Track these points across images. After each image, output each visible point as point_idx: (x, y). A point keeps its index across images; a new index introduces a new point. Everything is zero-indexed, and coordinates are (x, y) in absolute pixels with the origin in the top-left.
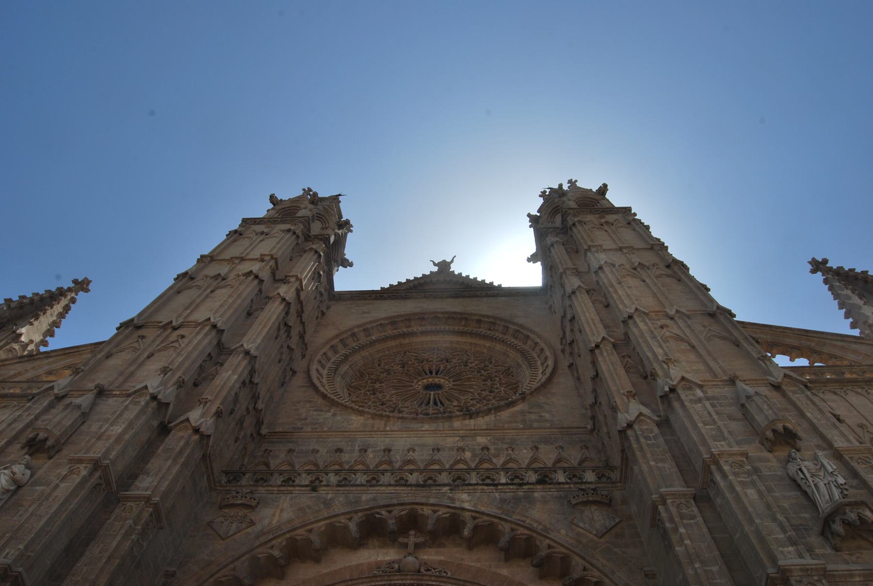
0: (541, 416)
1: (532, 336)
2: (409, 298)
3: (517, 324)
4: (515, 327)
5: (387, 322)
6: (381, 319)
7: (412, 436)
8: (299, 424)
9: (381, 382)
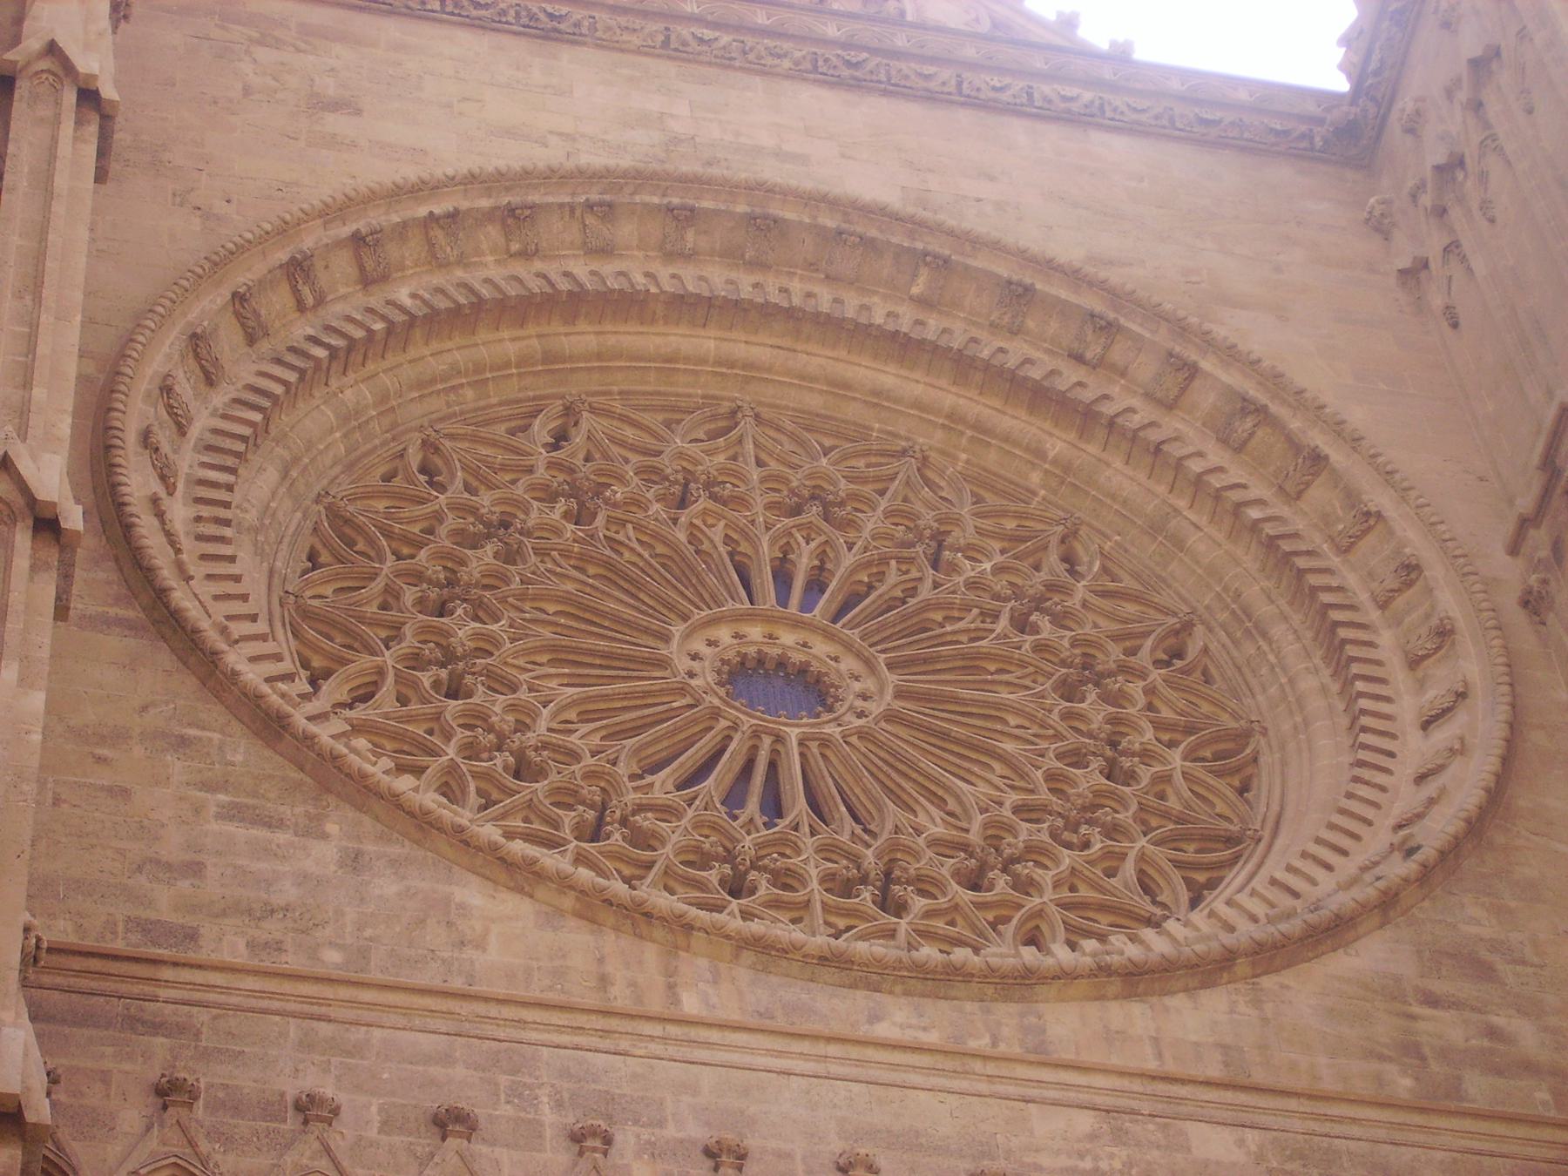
0: (1493, 1033)
1: (1337, 456)
2: (574, 38)
3: (1251, 365)
4: (1232, 378)
5: (485, 203)
6: (451, 181)
7: (835, 1069)
8: (164, 902)
9: (480, 612)
